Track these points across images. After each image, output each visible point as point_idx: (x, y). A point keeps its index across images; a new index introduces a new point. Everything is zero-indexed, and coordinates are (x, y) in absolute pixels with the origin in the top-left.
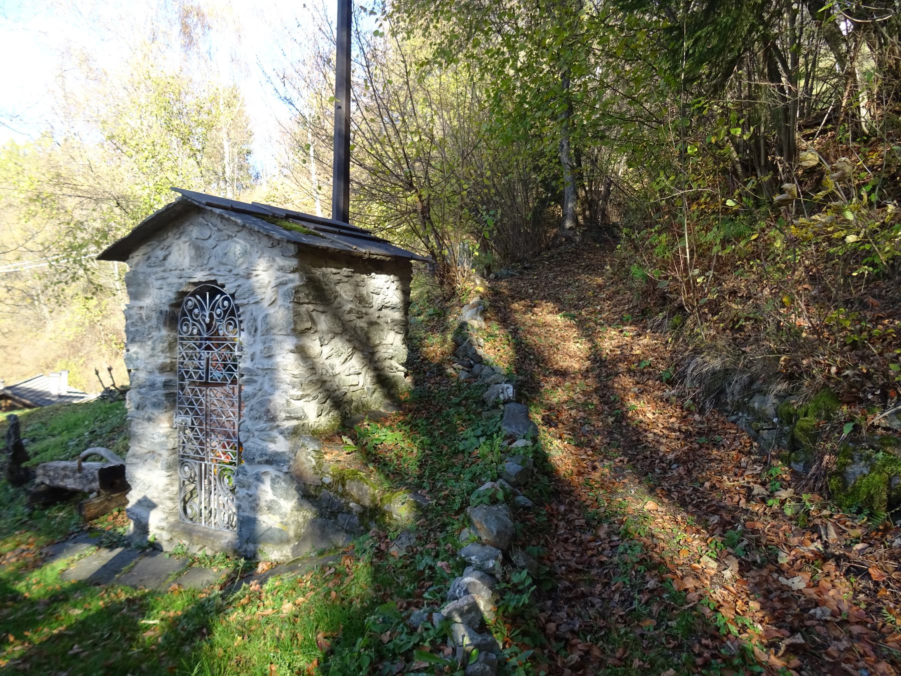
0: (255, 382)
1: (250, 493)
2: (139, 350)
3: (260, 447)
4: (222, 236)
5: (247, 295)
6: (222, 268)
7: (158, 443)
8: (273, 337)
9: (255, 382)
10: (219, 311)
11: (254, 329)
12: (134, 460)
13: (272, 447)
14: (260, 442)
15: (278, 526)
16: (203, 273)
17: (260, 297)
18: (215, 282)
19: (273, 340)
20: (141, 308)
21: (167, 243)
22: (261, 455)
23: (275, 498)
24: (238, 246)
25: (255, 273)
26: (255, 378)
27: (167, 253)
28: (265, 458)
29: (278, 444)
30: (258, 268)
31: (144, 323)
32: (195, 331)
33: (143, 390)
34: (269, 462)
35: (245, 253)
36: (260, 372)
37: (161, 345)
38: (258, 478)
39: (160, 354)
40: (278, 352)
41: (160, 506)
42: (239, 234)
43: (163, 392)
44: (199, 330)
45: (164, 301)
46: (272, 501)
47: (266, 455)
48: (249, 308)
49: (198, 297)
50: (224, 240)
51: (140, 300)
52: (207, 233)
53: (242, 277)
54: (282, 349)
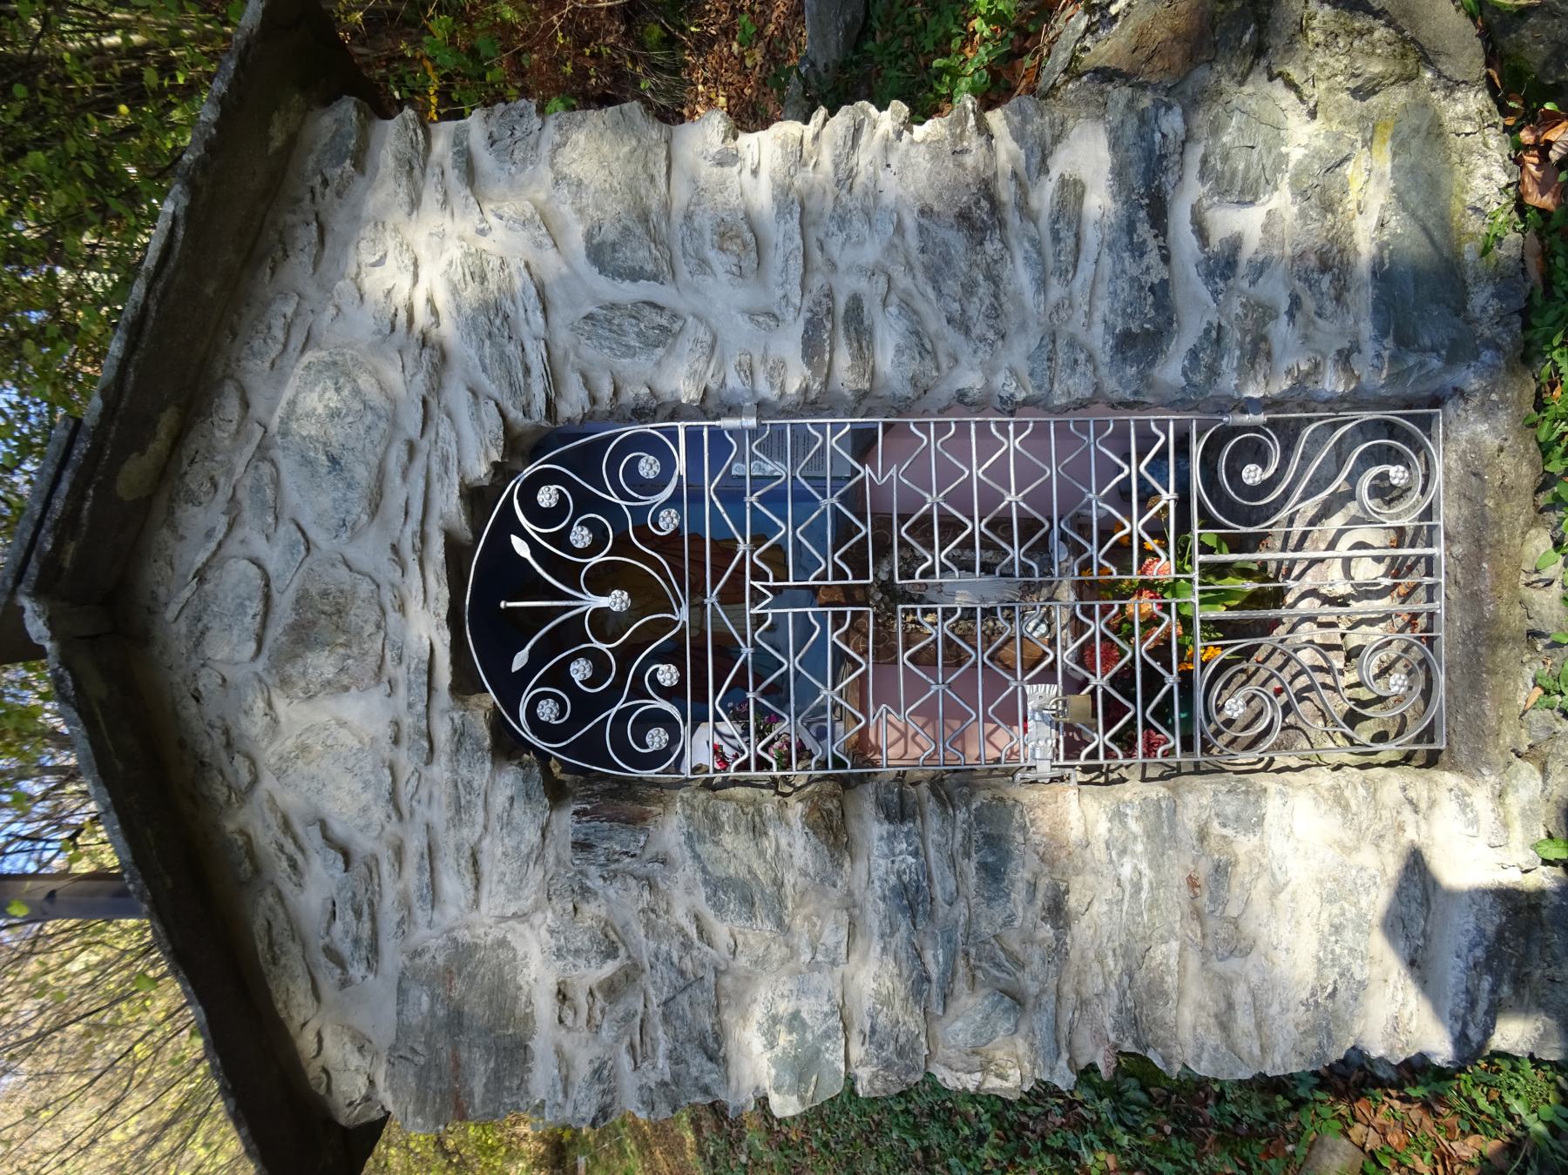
0: (856, 304)
1: (1284, 305)
2: (758, 1013)
3: (1107, 260)
4: (257, 489)
5: (511, 349)
6: (397, 493)
7: (1155, 865)
8: (677, 219)
9: (856, 304)
10: (581, 537)
11: (647, 311)
12: (1244, 1021)
13: (1099, 202)
14: (1086, 268)
15: (1383, 159)
16: (415, 606)
17: (520, 281)
18: (456, 553)
19: (688, 217)
20: (562, 996)
21: (266, 837)
22: (1138, 251)
23: (1284, 182)
24: (303, 398)
25: (422, 317)
26: (841, 303)
27: (313, 839)
28: (1144, 231)
29: (1085, 174)
30: (400, 299)
31: (630, 975)
32: (667, 674)
33: (934, 960)
34: (1158, 211)
35: (337, 370)
36: (817, 281)
37: (727, 839)
38: (1223, 265)
39: (768, 845)
40: (734, 201)
41: (1410, 834)
42: (258, 408)
43: (934, 823)
44: (660, 656)
45: (532, 835)
46: (1302, 194)
47: (1131, 228)
48: (563, 338)
49: (520, 660)
50: (277, 483)
51: (528, 1019)
52: (237, 577)
53: (436, 386)
54: (722, 186)
